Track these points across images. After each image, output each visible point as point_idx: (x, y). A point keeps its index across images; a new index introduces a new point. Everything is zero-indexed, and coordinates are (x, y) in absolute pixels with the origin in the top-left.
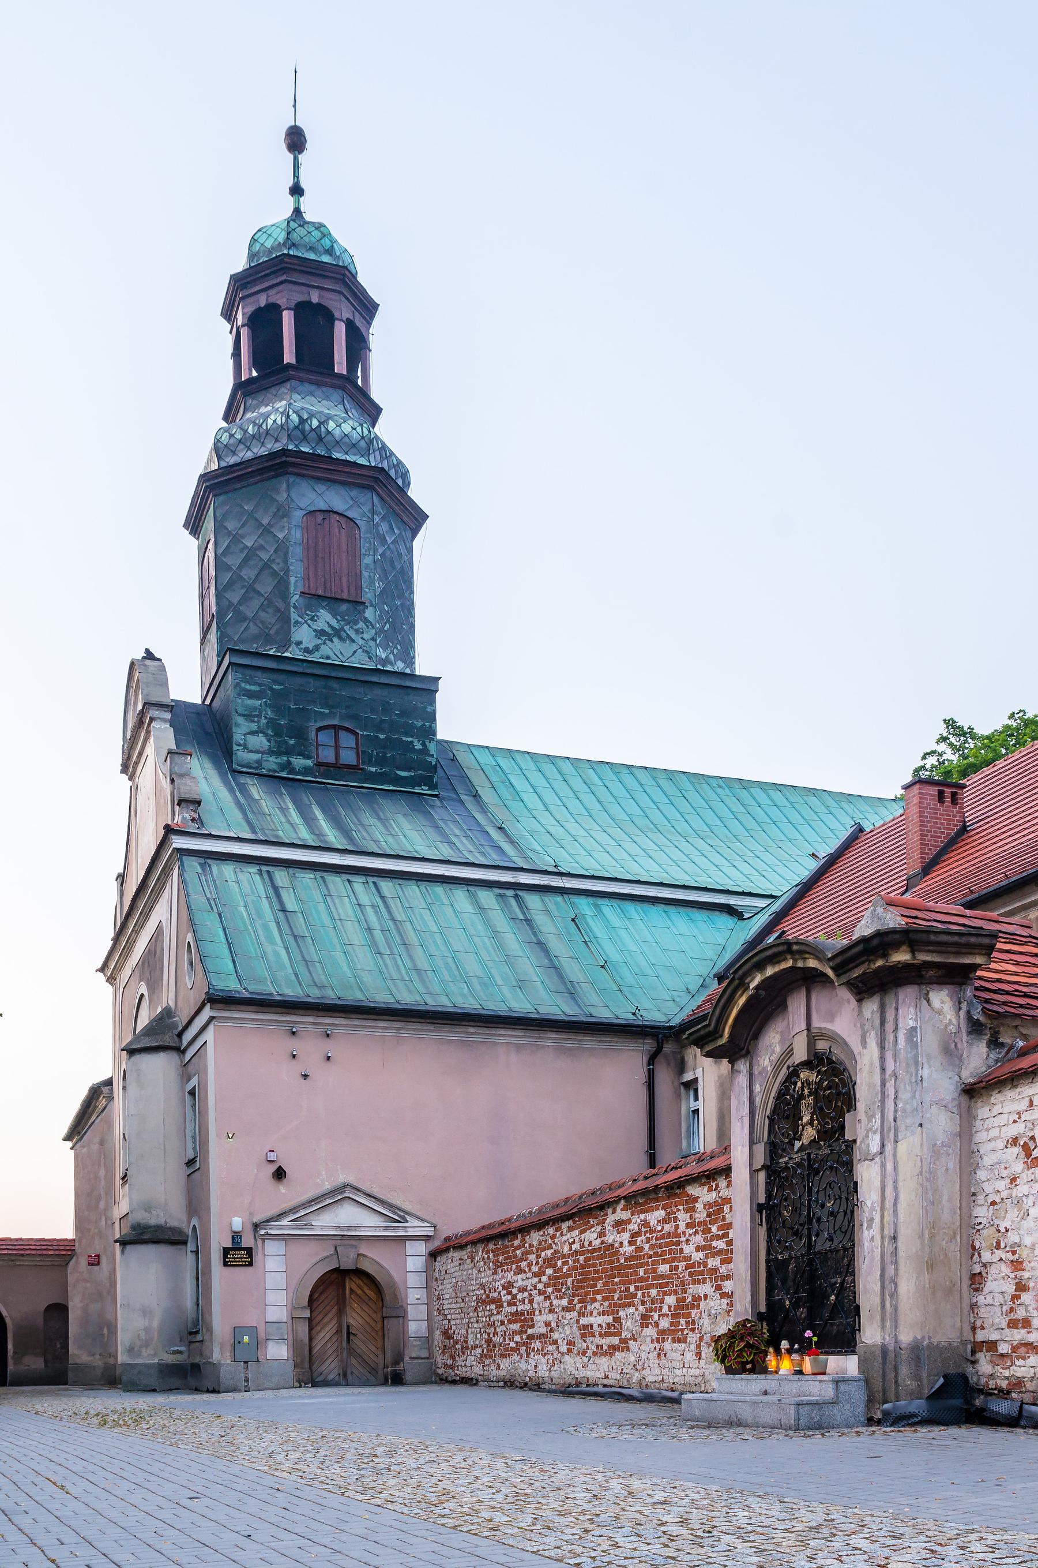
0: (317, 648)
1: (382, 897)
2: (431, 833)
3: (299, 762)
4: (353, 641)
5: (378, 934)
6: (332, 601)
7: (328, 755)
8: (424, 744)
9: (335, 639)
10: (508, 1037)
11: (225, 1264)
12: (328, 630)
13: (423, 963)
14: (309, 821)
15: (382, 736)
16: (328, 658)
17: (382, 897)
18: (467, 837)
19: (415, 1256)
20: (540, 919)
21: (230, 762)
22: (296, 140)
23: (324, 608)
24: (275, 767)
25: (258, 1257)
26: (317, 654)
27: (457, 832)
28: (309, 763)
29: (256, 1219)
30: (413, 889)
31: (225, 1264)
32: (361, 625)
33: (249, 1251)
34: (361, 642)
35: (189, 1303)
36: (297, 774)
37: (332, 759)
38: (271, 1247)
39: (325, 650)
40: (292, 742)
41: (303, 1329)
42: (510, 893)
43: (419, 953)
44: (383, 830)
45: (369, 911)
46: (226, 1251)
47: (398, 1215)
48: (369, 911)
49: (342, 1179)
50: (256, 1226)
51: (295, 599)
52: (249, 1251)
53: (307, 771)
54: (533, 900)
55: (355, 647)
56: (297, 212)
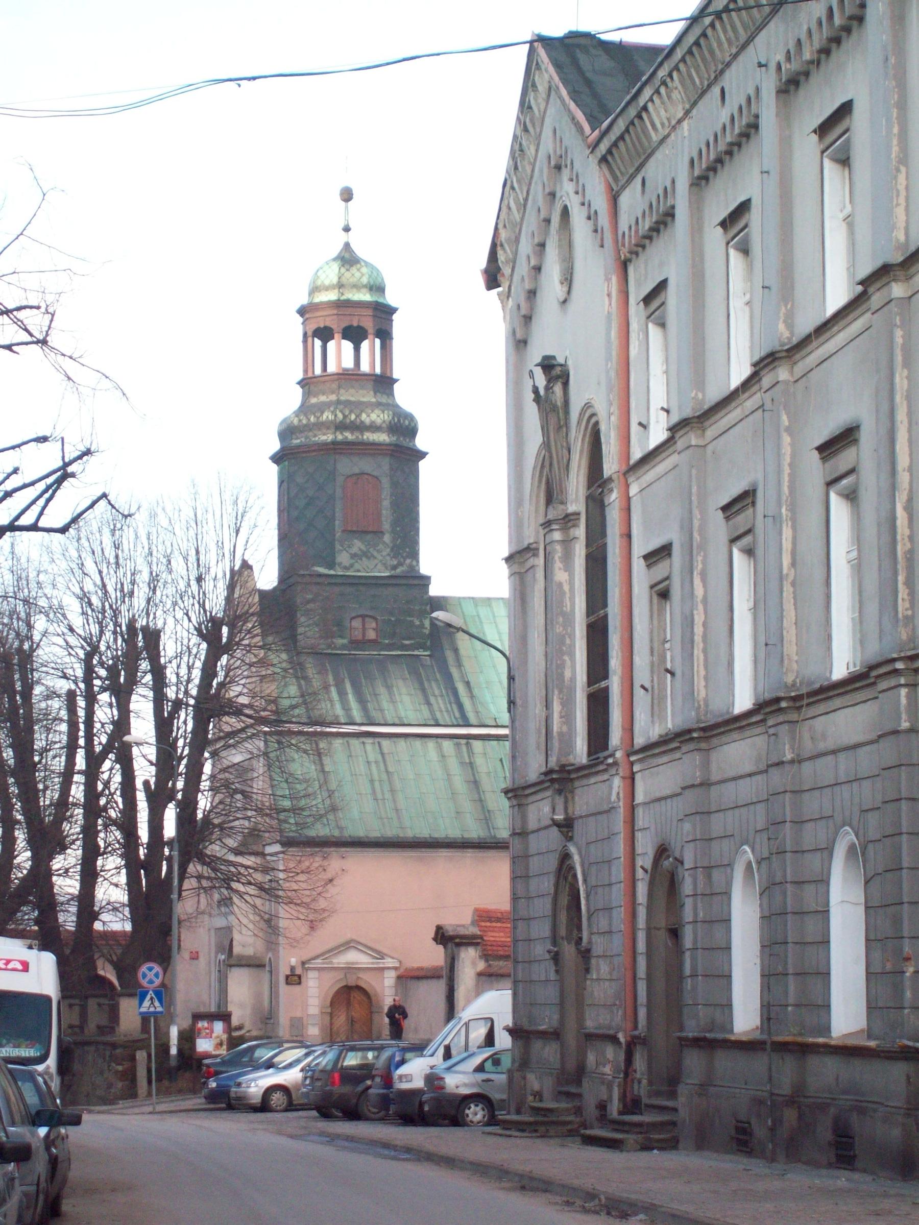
0: (352, 566)
1: (382, 754)
2: (421, 698)
3: (340, 641)
4: (375, 558)
5: (377, 784)
6: (361, 533)
7: (358, 635)
8: (421, 621)
9: (364, 559)
10: (444, 853)
11: (287, 983)
12: (359, 553)
13: (402, 804)
14: (342, 694)
15: (393, 619)
16: (359, 571)
17: (382, 754)
18: (442, 696)
19: (389, 979)
20: (479, 761)
21: (295, 647)
22: (347, 195)
23: (356, 538)
24: (323, 646)
25: (303, 980)
26: (352, 570)
27: (437, 692)
28: (345, 641)
29: (304, 959)
30: (402, 743)
31: (287, 983)
32: (381, 546)
33: (299, 977)
34: (381, 558)
35: (266, 1003)
36: (339, 649)
37: (360, 637)
38: (311, 974)
39: (357, 566)
40: (335, 629)
41: (328, 1018)
42: (463, 741)
43: (400, 796)
44: (388, 696)
45: (374, 767)
46: (287, 977)
47: (382, 956)
48: (374, 767)
49: (349, 936)
50: (303, 963)
51: (338, 535)
52: (299, 977)
53: (343, 647)
54: (477, 745)
55: (376, 561)
56: (347, 245)
